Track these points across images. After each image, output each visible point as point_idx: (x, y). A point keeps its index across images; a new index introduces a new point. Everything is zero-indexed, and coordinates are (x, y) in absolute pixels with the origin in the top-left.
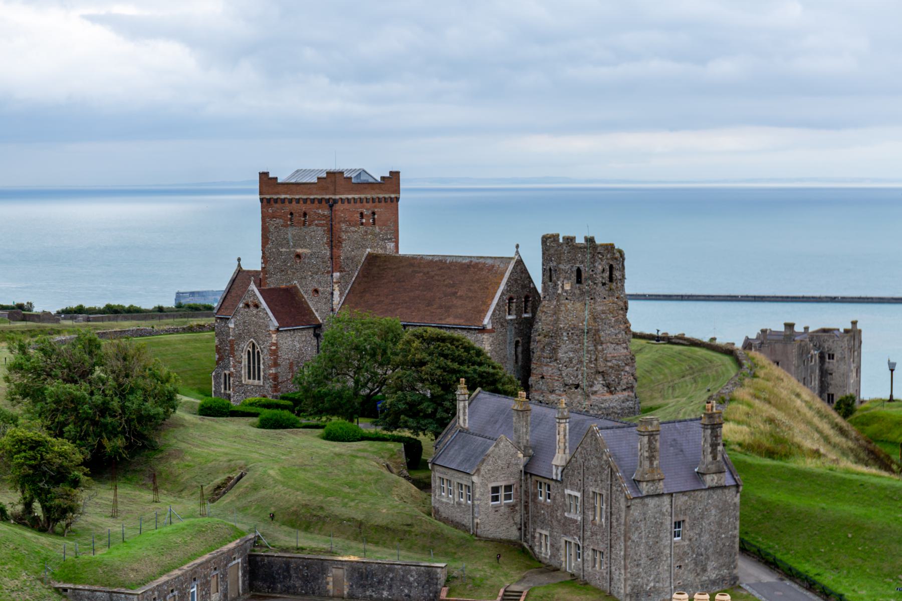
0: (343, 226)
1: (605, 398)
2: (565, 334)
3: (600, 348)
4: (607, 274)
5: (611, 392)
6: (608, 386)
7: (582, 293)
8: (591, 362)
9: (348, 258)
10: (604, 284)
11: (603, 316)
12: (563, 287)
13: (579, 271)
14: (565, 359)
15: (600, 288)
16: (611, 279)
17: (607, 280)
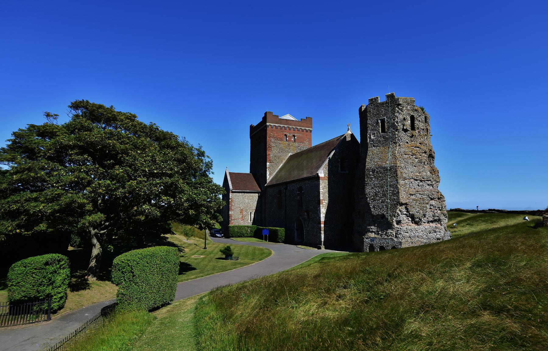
0: (273, 140)
1: (410, 227)
2: (371, 173)
3: (401, 182)
4: (409, 122)
5: (417, 223)
6: (412, 217)
7: (386, 139)
8: (394, 194)
9: (275, 156)
10: (406, 131)
11: (406, 156)
12: (370, 138)
13: (383, 121)
14: (371, 194)
15: (402, 134)
16: (413, 127)
17: (409, 128)
